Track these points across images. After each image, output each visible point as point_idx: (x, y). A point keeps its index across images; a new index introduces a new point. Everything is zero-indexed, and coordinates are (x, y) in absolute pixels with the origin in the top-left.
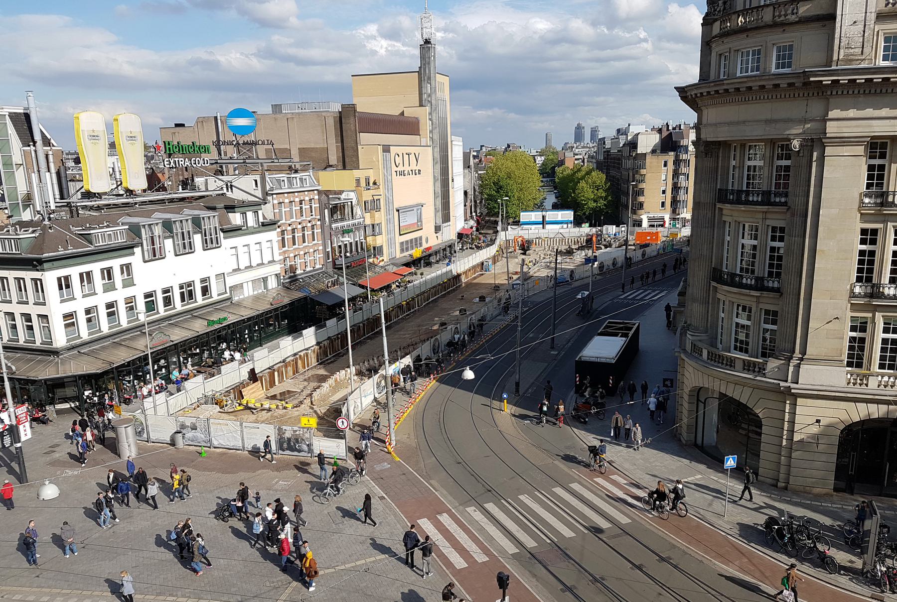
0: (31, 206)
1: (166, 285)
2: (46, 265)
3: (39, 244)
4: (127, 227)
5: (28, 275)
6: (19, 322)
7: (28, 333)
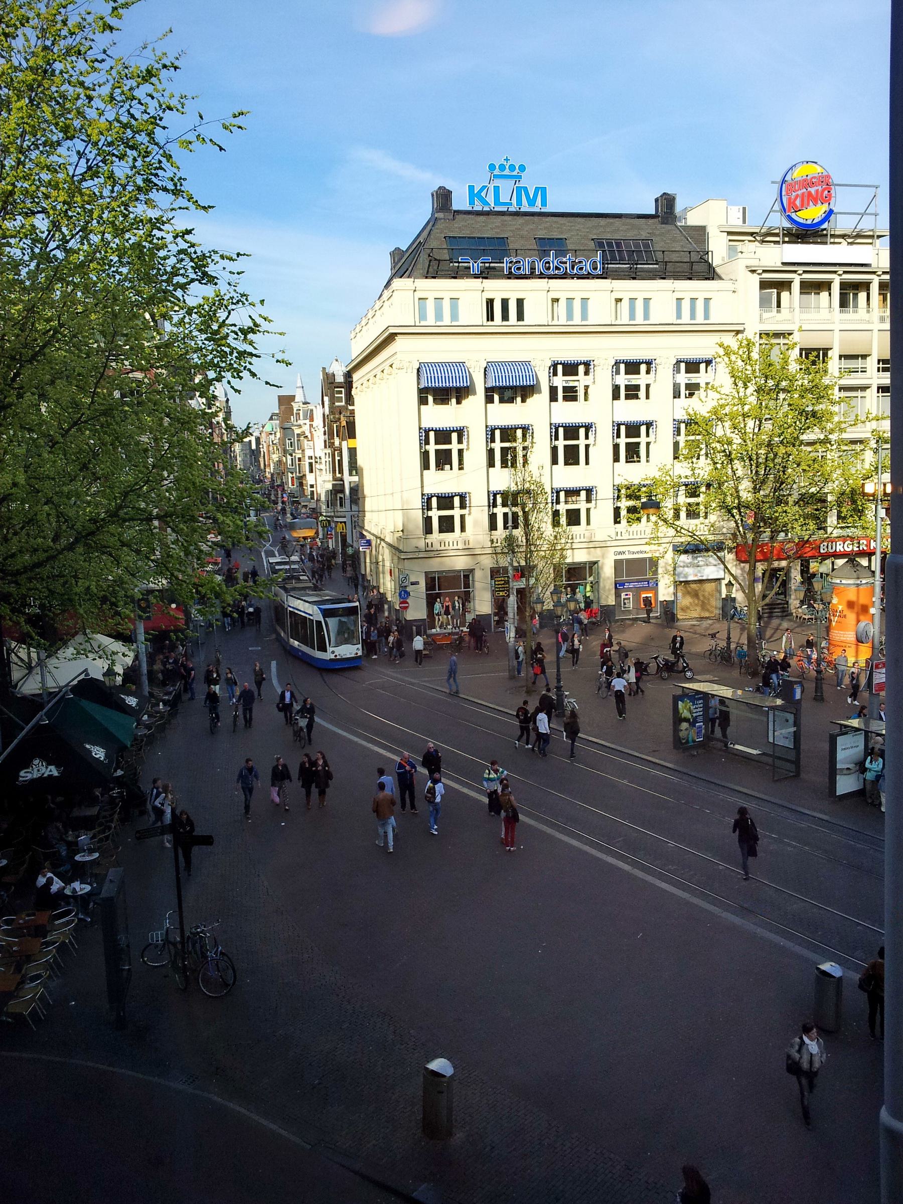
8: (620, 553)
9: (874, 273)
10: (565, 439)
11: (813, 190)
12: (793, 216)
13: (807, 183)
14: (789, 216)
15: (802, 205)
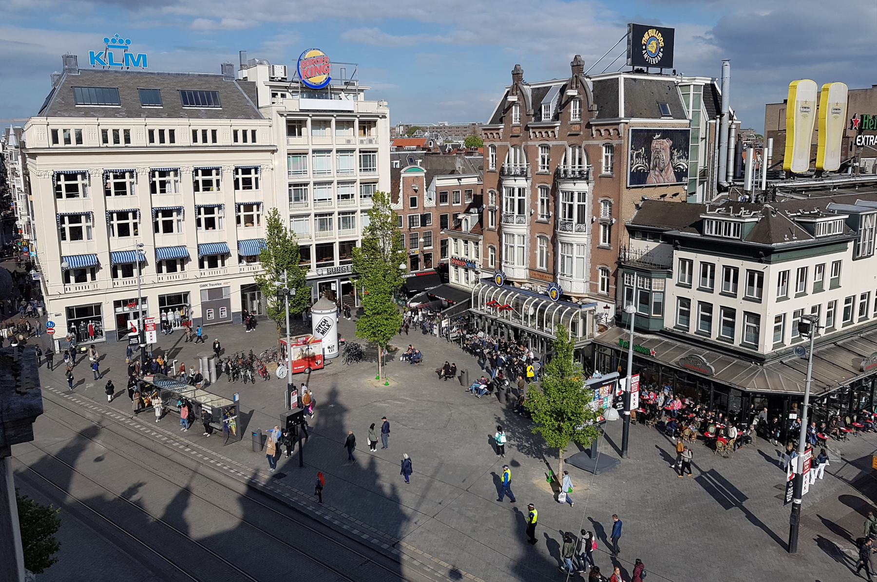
0: (706, 183)
1: (865, 291)
2: (773, 257)
3: (763, 229)
4: (847, 216)
5: (744, 266)
6: (717, 316)
7: (640, 306)
8: (204, 286)
9: (356, 116)
10: (205, 214)
11: (318, 66)
12: (306, 81)
13: (315, 61)
14: (303, 81)
15: (312, 75)
